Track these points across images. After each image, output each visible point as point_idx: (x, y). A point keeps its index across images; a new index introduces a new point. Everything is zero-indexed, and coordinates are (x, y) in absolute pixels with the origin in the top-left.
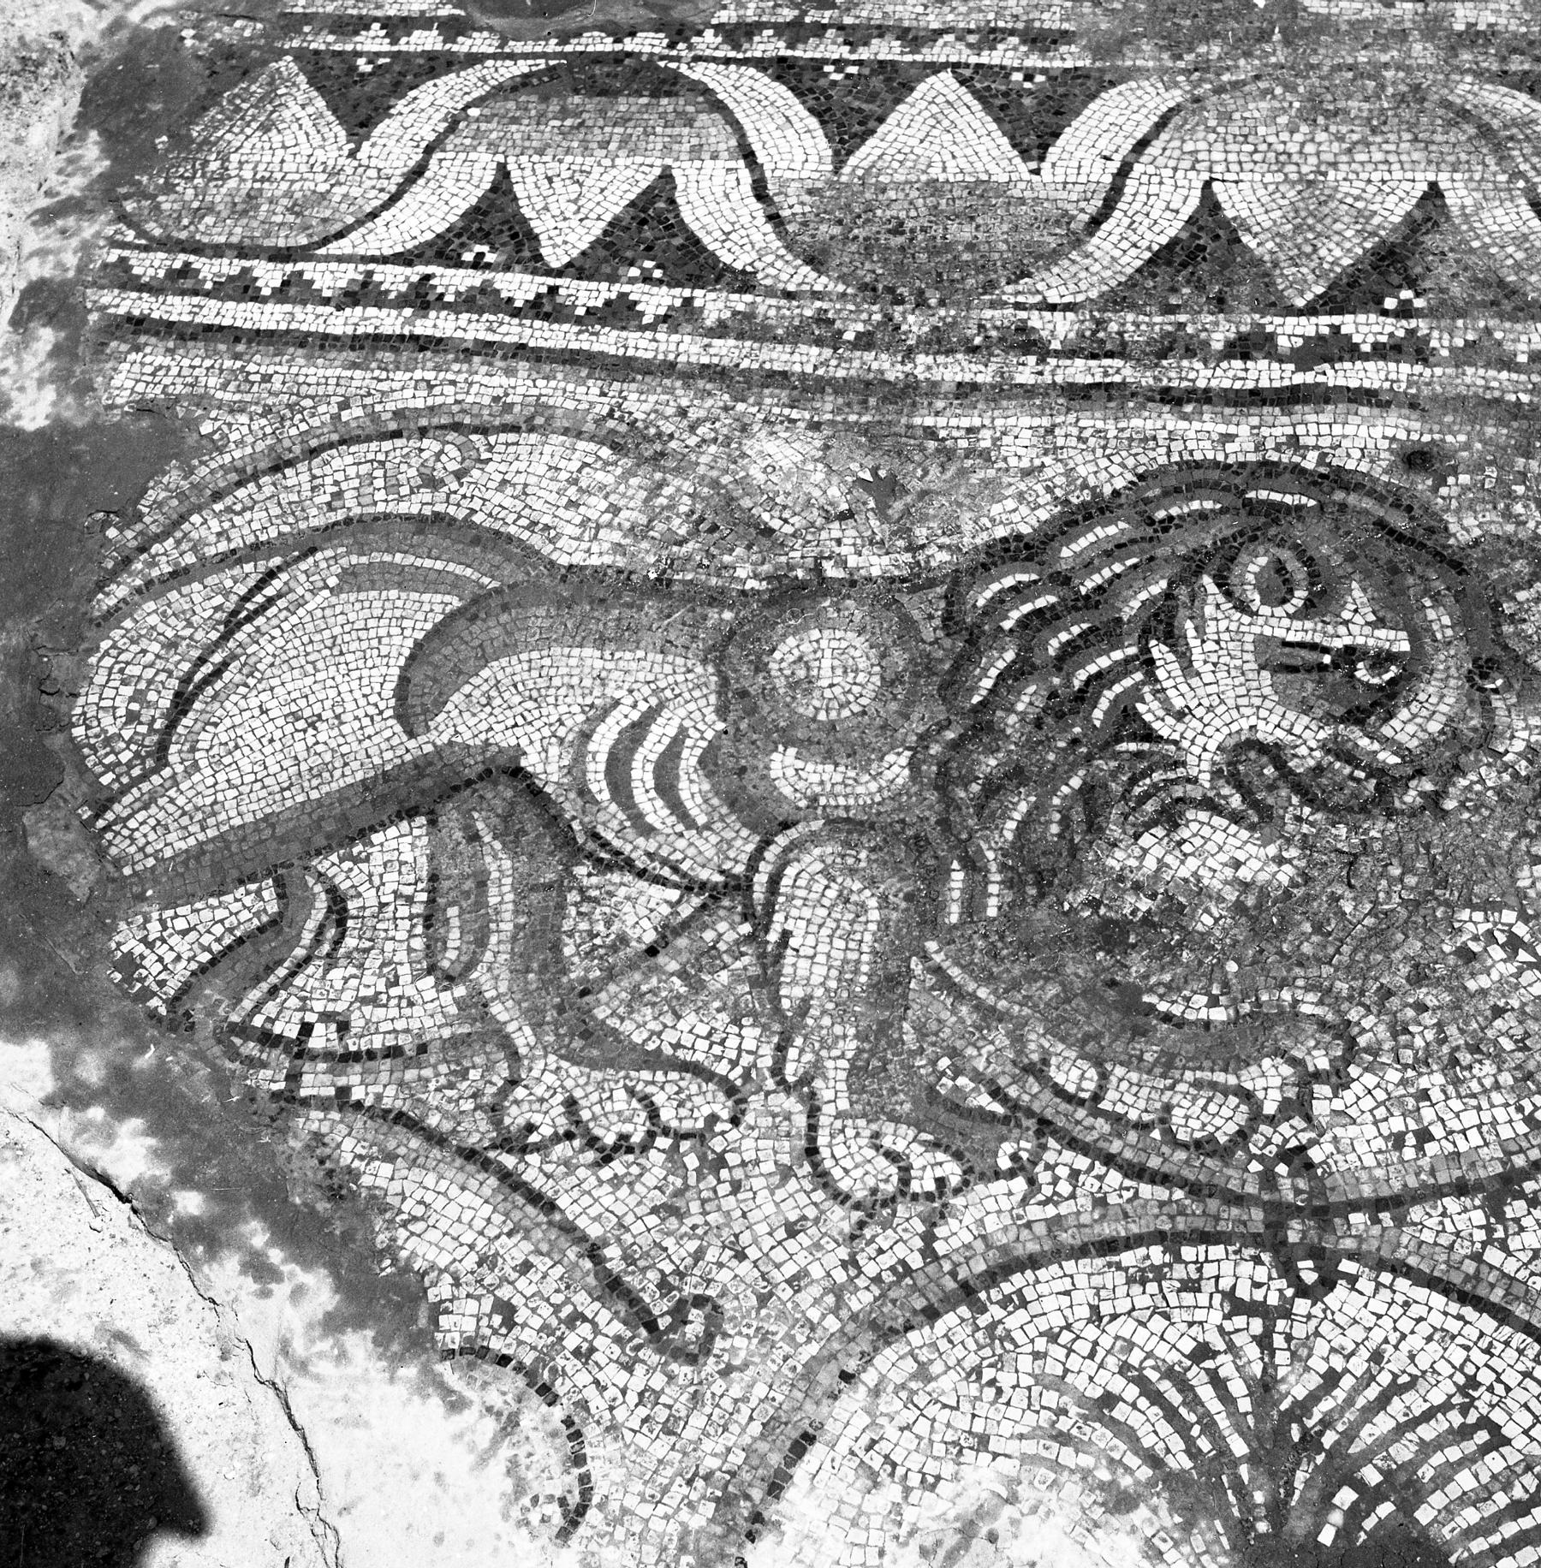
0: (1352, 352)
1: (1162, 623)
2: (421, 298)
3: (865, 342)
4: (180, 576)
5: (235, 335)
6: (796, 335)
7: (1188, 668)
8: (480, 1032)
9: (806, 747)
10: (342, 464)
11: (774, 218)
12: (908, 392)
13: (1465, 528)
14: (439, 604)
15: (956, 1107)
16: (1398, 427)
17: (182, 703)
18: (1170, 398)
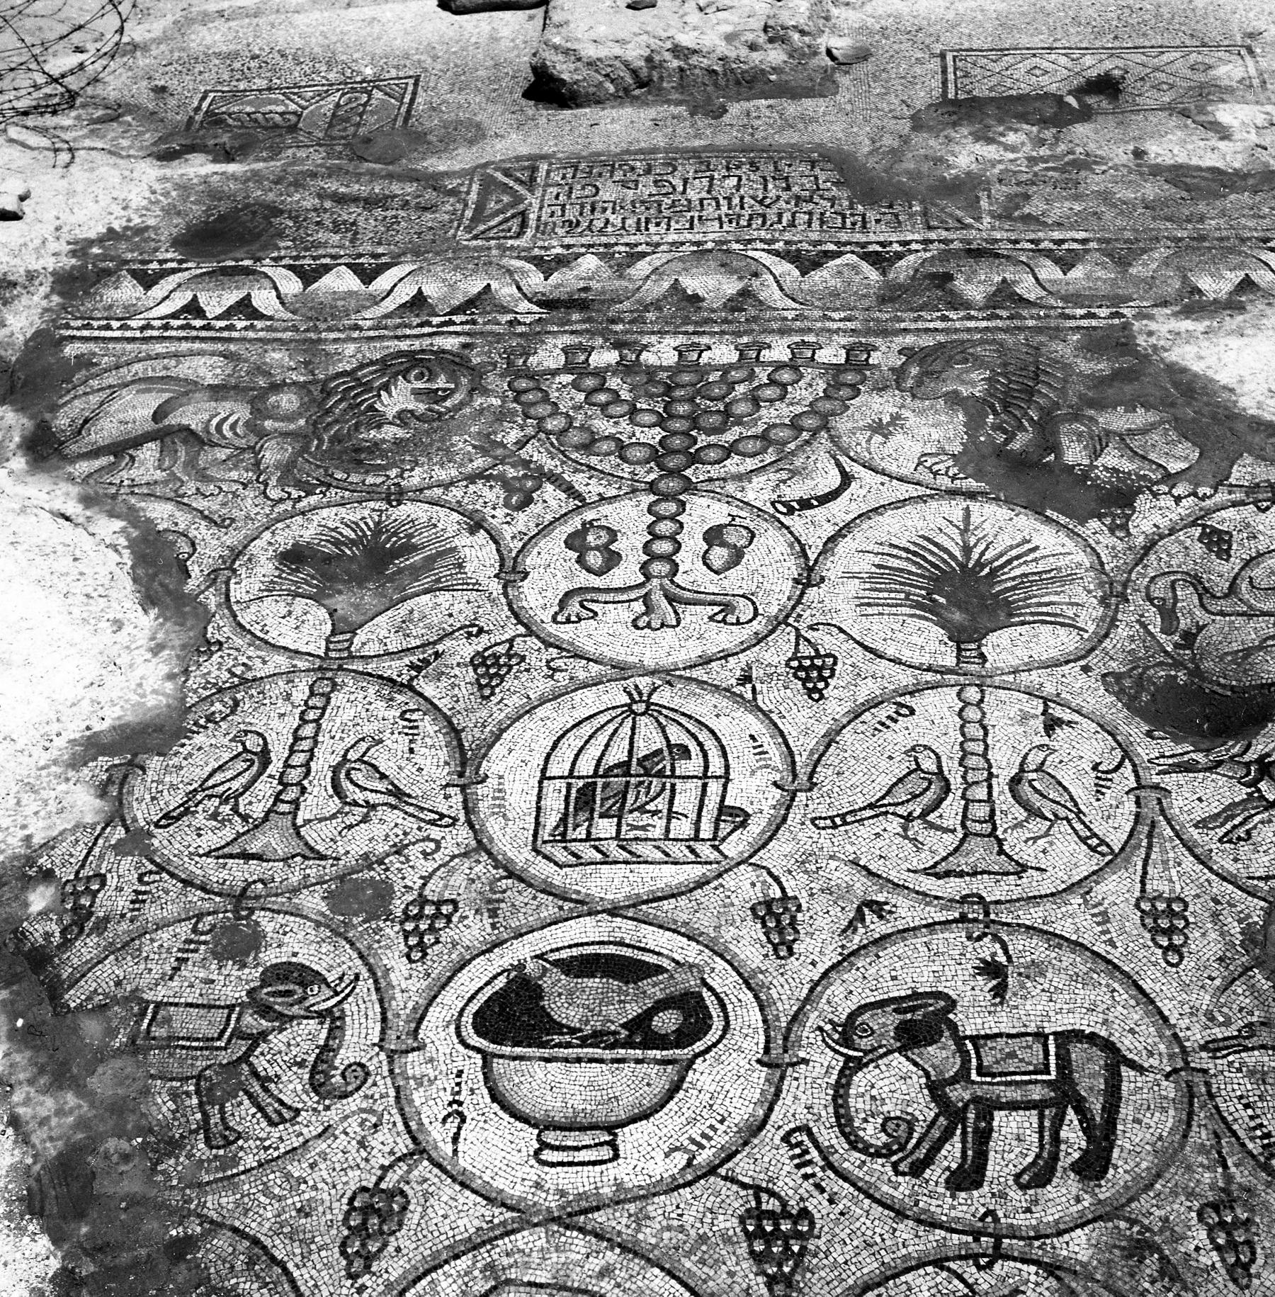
0: (454, 323)
1: (386, 387)
2: (166, 327)
3: (307, 330)
4: (86, 394)
5: (104, 339)
6: (285, 330)
7: (390, 395)
8: (173, 477)
9: (276, 419)
10: (137, 367)
11: (282, 303)
12: (319, 341)
13: (476, 361)
14: (167, 396)
15: (307, 482)
16: (462, 339)
17: (86, 421)
18: (398, 338)
